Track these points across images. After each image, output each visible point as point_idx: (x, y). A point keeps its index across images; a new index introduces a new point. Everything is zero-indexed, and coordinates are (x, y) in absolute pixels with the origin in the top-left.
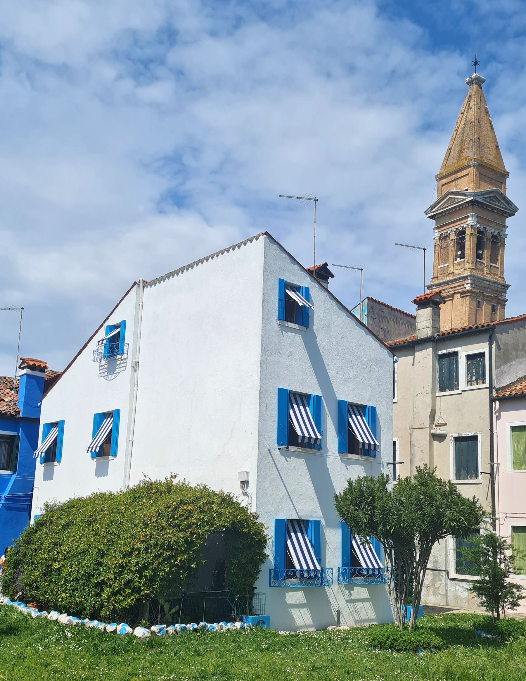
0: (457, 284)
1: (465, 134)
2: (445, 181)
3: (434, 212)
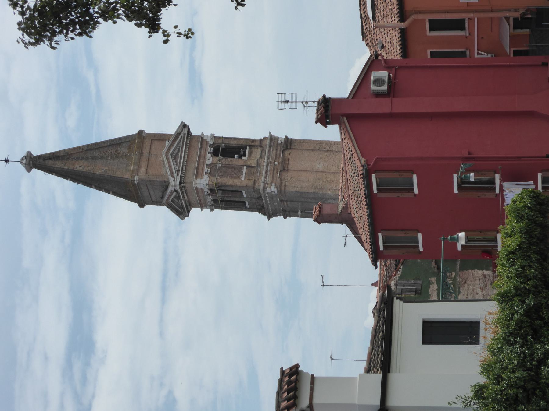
0: (275, 151)
1: (97, 154)
3: (178, 175)
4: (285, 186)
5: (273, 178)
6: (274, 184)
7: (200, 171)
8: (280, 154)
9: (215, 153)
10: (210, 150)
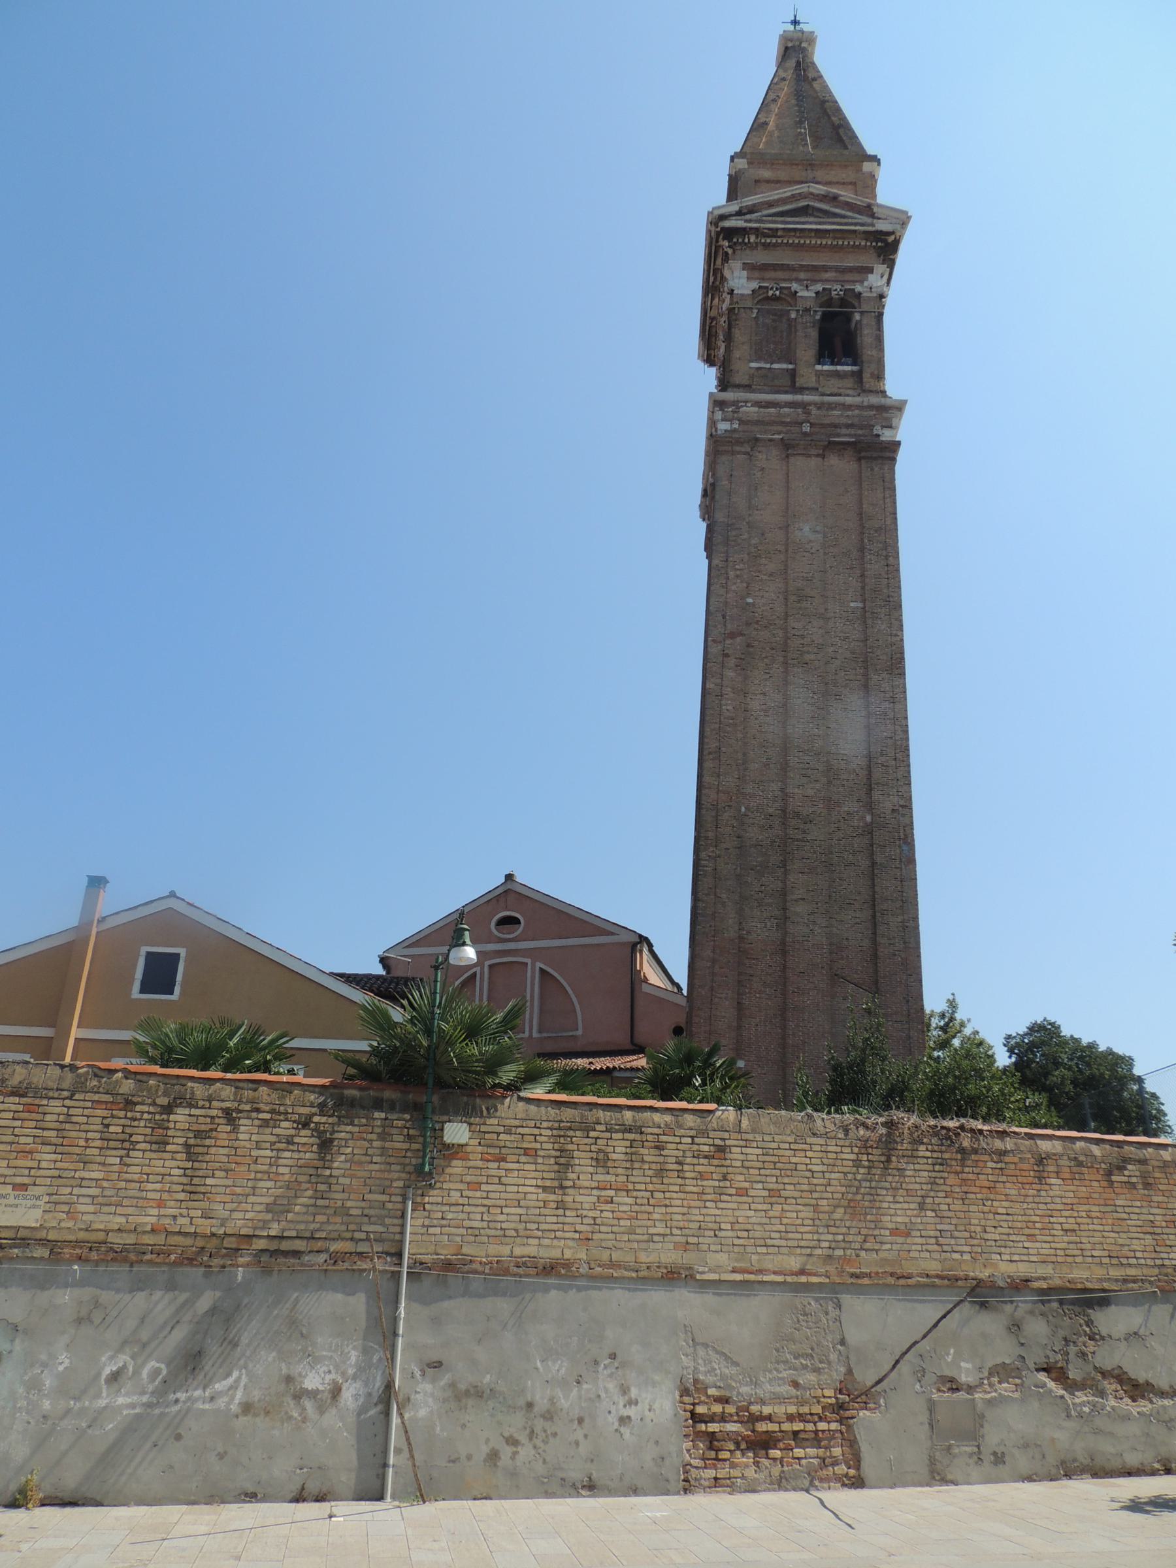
3: (746, 221)
4: (733, 453)
5: (758, 423)
6: (736, 426)
7: (772, 274)
10: (836, 289)
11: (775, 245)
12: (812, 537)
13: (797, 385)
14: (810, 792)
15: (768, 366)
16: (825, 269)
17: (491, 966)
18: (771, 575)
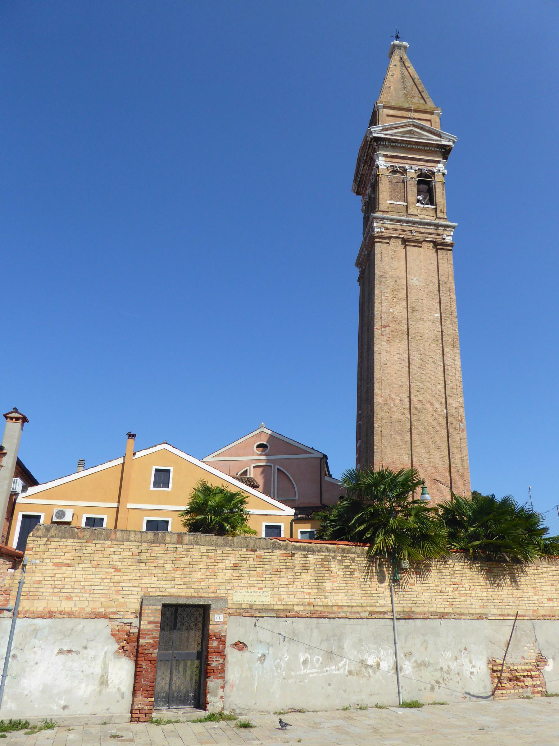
0: (430, 231)
2: (391, 112)
8: (428, 238)
9: (421, 174)
11: (397, 147)
12: (417, 283)
13: (409, 213)
14: (421, 399)
15: (395, 203)
16: (420, 160)
17: (255, 467)
18: (400, 300)
